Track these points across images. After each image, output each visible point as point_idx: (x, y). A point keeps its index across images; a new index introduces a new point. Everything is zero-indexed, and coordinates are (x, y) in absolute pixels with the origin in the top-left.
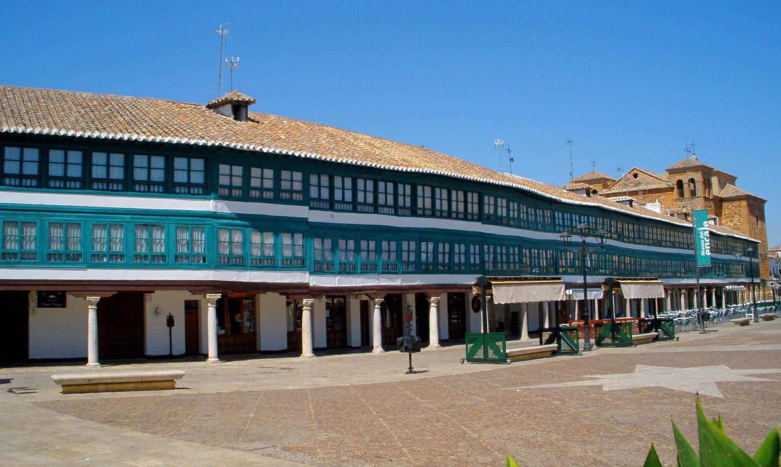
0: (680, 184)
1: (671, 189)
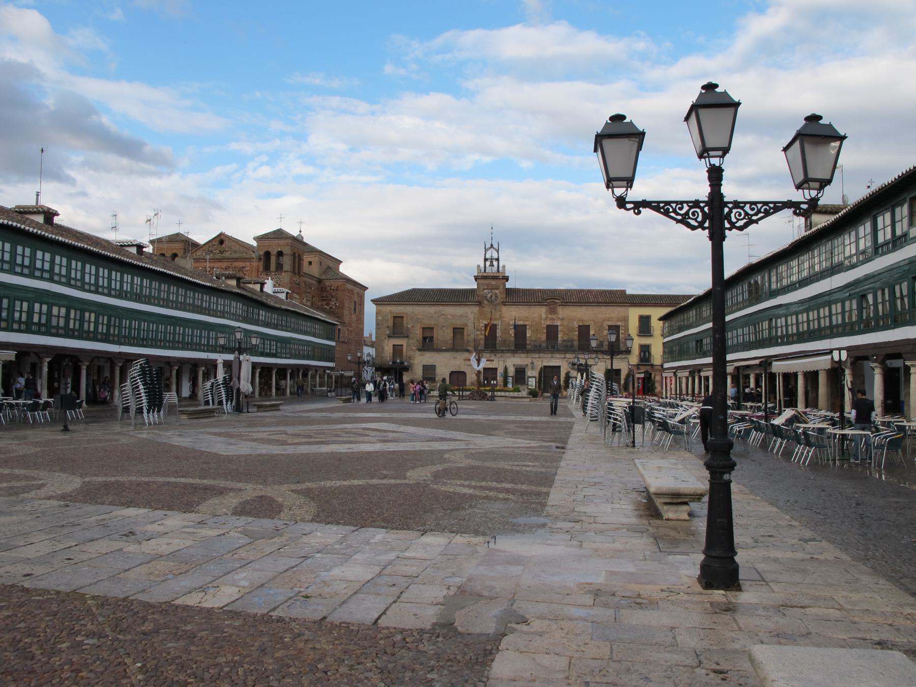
0: (267, 254)
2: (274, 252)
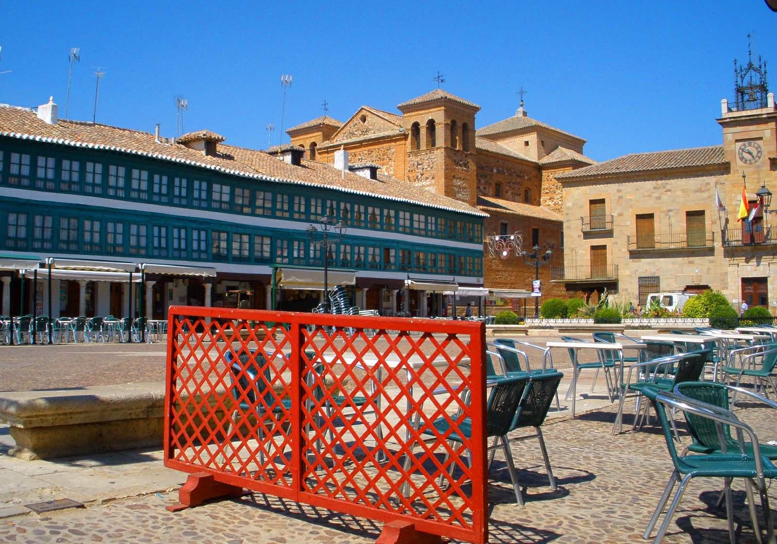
1: (405, 137)
2: (423, 124)
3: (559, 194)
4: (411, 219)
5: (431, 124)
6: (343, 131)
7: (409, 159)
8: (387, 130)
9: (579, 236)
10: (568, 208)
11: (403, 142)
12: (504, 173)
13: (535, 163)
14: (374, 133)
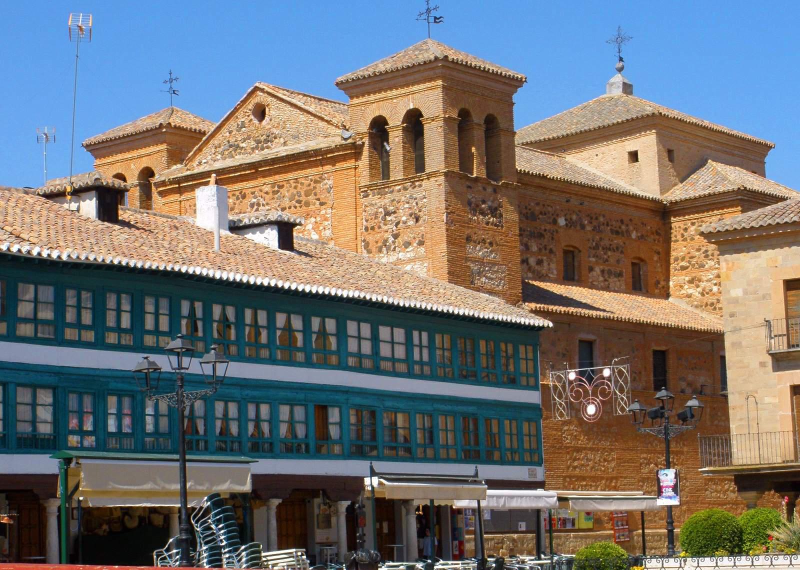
1: (355, 151)
3: (711, 268)
4: (375, 339)
5: (414, 122)
6: (215, 141)
7: (365, 201)
8: (316, 136)
9: (763, 365)
10: (735, 301)
11: (351, 163)
12: (583, 227)
13: (654, 201)
14: (285, 144)
